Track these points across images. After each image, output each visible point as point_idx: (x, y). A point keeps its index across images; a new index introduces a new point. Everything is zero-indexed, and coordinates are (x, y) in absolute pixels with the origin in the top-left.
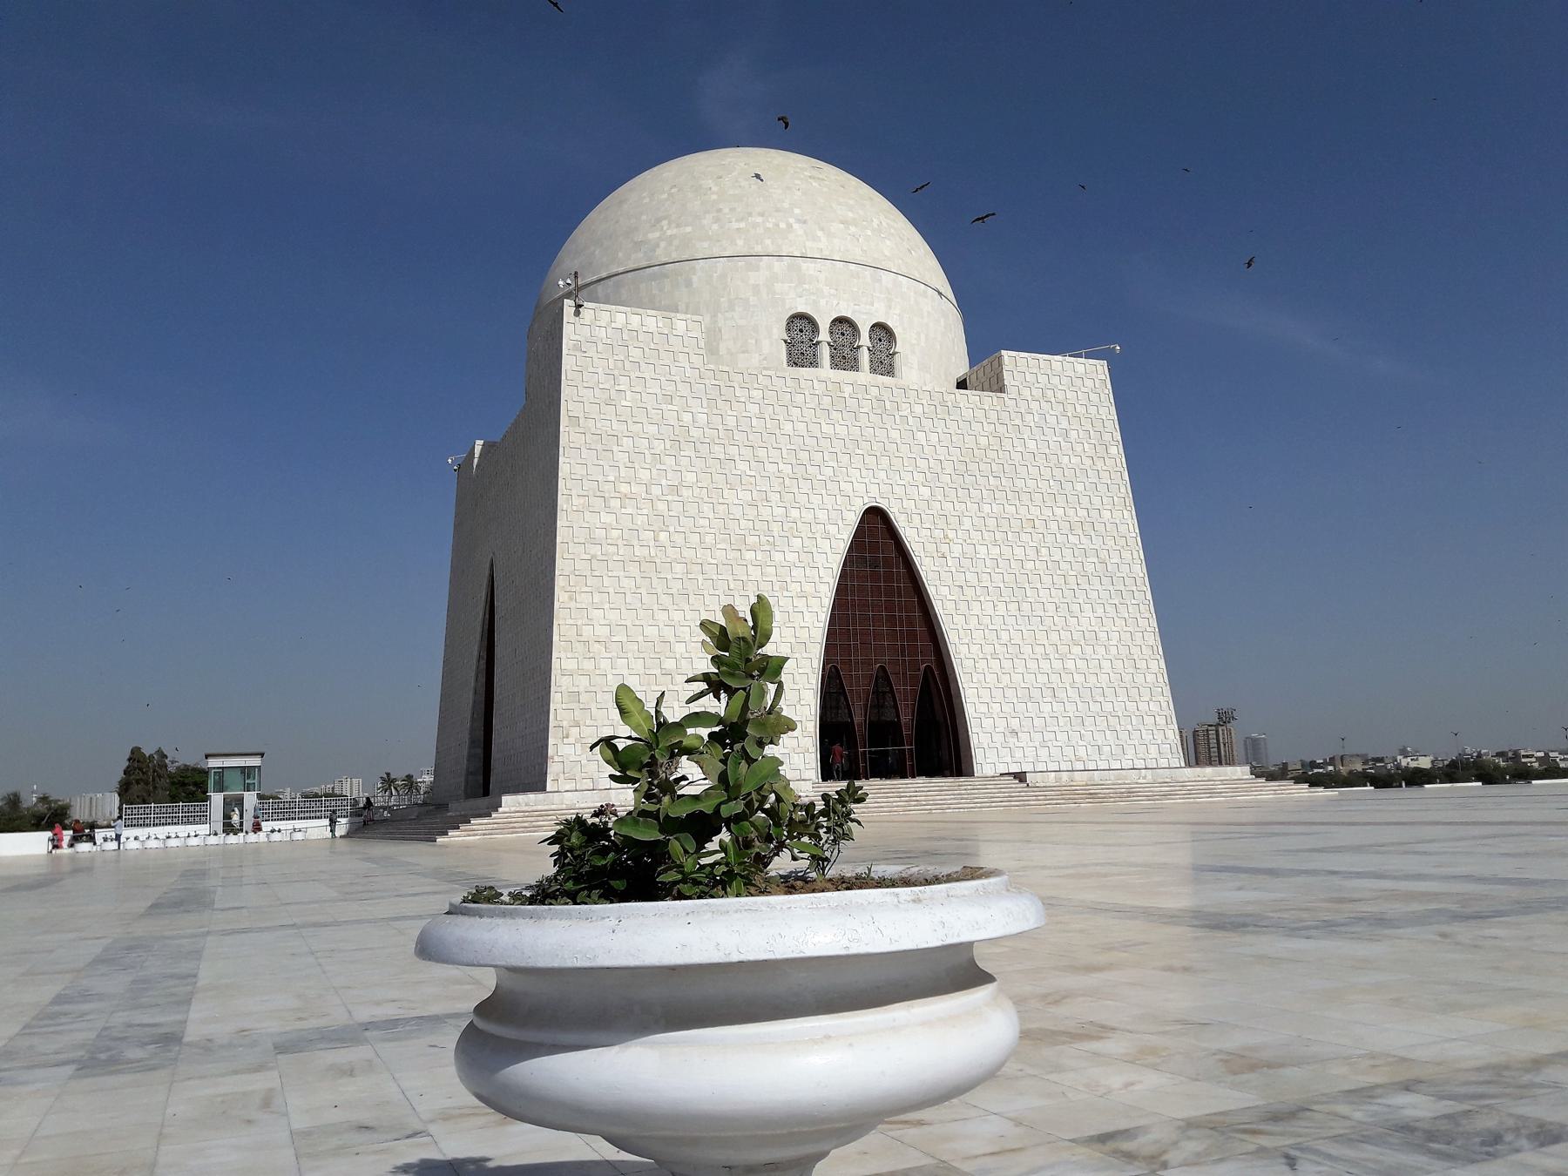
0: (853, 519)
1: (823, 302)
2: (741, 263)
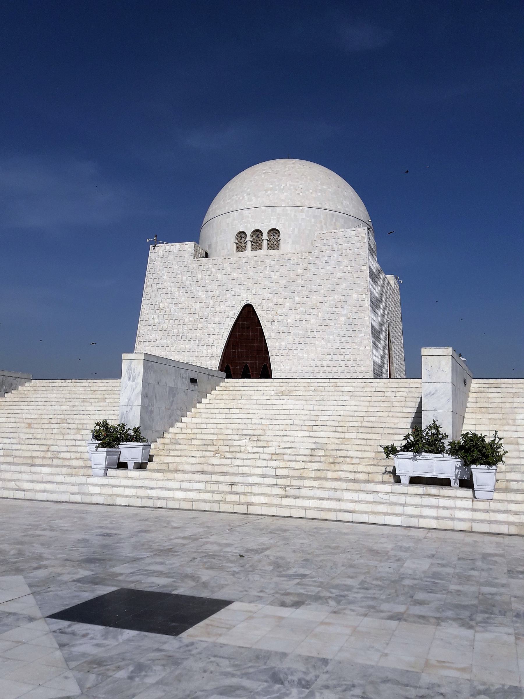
0: (239, 309)
1: (249, 225)
2: (225, 216)
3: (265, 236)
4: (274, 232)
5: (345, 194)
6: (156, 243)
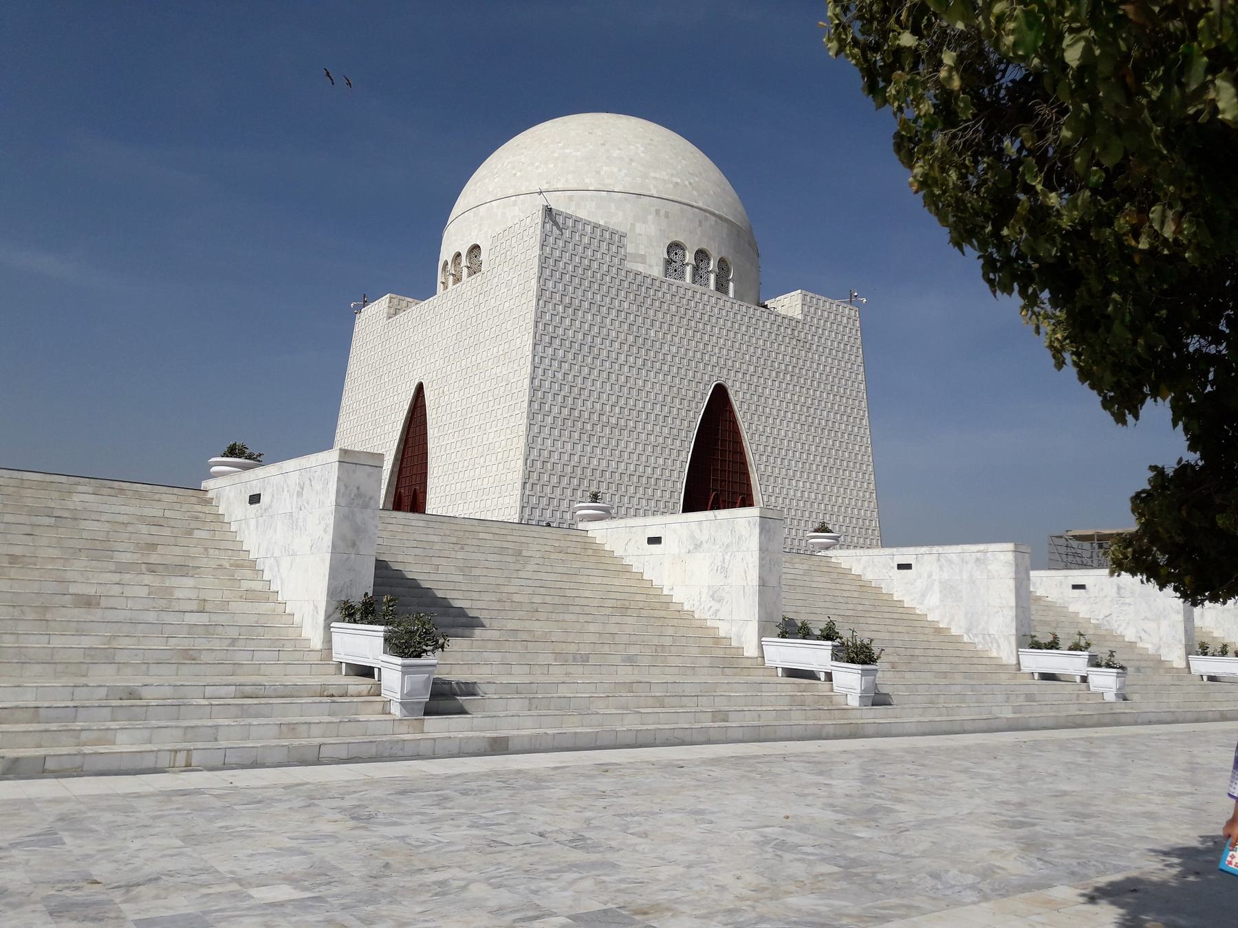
3: (464, 261)
4: (475, 248)
5: (616, 153)
6: (365, 303)
